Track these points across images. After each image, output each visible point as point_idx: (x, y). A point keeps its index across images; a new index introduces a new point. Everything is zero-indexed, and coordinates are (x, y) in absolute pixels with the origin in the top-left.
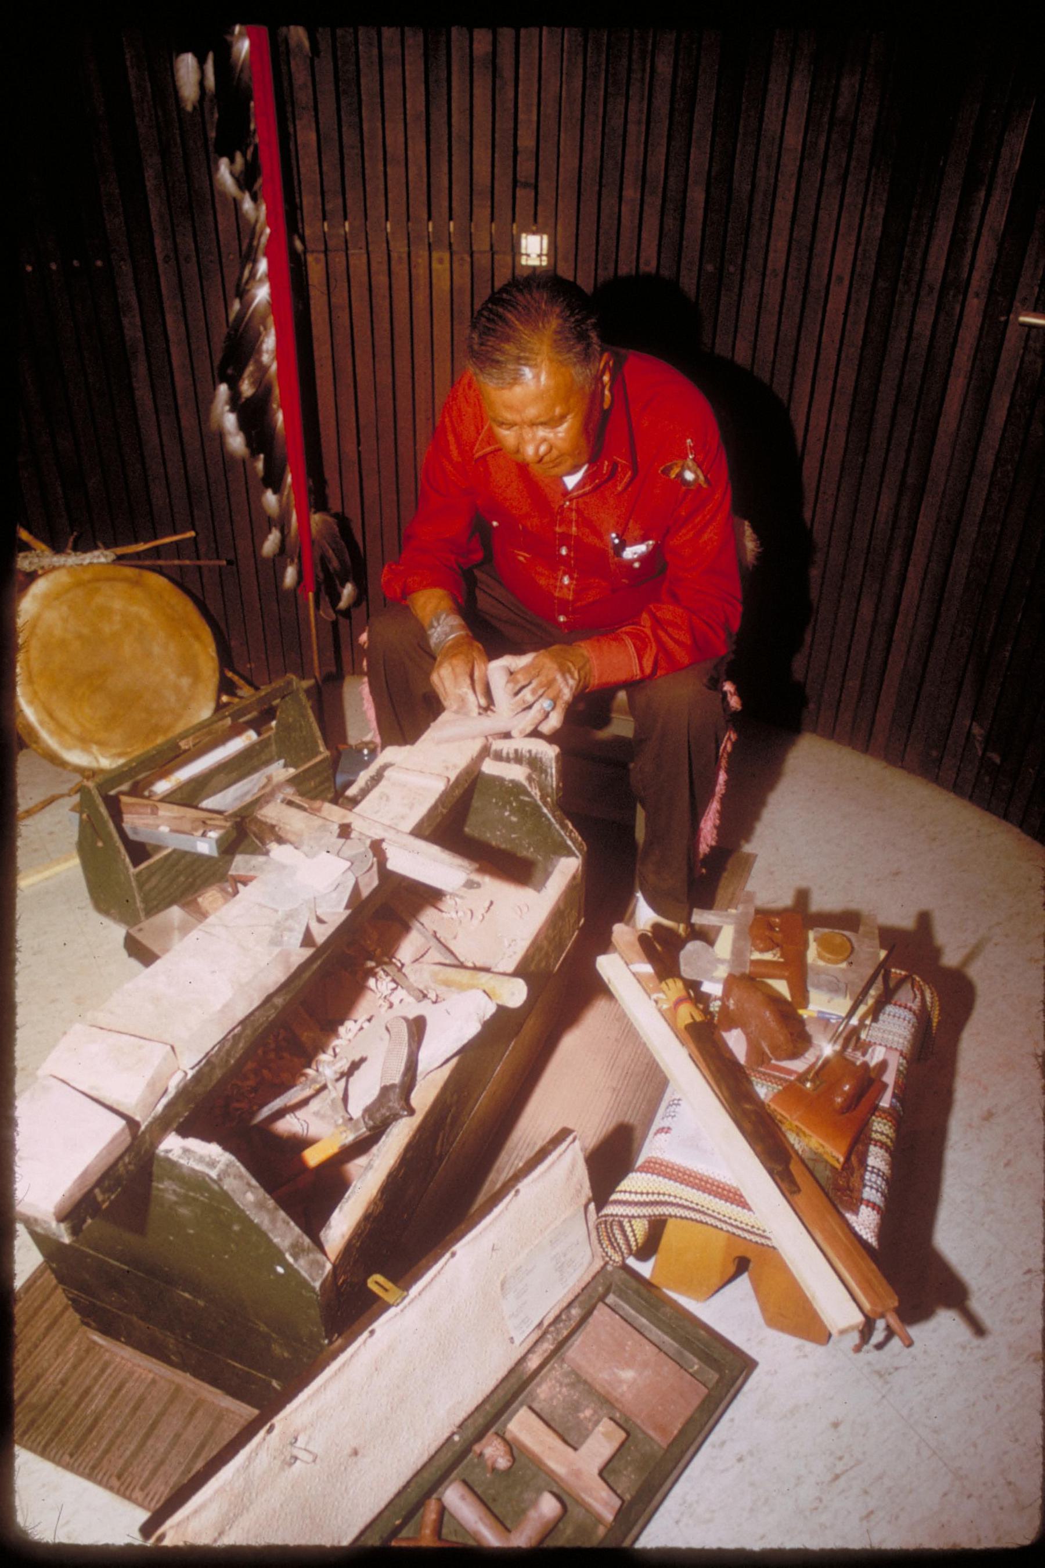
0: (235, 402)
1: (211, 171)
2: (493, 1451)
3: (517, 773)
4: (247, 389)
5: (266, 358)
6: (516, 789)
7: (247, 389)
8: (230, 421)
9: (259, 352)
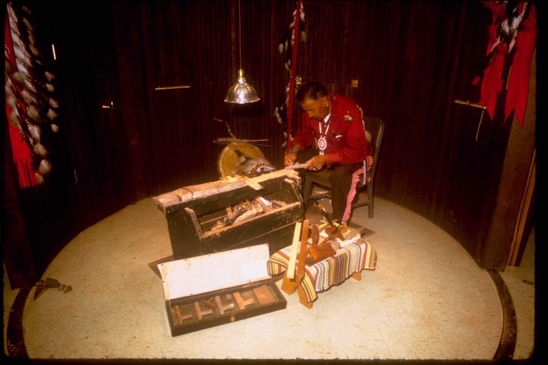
0: (279, 112)
1: (284, 65)
2: (229, 297)
3: (291, 182)
4: (282, 108)
5: (286, 103)
6: (289, 185)
7: (282, 108)
8: (278, 115)
9: (285, 101)
